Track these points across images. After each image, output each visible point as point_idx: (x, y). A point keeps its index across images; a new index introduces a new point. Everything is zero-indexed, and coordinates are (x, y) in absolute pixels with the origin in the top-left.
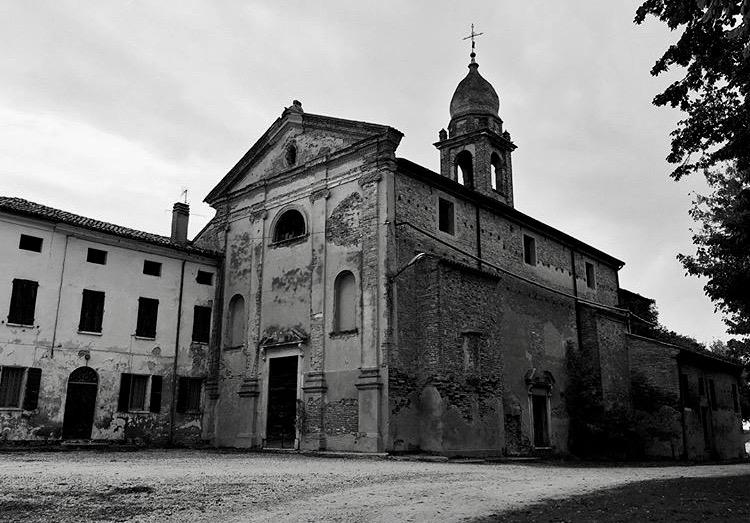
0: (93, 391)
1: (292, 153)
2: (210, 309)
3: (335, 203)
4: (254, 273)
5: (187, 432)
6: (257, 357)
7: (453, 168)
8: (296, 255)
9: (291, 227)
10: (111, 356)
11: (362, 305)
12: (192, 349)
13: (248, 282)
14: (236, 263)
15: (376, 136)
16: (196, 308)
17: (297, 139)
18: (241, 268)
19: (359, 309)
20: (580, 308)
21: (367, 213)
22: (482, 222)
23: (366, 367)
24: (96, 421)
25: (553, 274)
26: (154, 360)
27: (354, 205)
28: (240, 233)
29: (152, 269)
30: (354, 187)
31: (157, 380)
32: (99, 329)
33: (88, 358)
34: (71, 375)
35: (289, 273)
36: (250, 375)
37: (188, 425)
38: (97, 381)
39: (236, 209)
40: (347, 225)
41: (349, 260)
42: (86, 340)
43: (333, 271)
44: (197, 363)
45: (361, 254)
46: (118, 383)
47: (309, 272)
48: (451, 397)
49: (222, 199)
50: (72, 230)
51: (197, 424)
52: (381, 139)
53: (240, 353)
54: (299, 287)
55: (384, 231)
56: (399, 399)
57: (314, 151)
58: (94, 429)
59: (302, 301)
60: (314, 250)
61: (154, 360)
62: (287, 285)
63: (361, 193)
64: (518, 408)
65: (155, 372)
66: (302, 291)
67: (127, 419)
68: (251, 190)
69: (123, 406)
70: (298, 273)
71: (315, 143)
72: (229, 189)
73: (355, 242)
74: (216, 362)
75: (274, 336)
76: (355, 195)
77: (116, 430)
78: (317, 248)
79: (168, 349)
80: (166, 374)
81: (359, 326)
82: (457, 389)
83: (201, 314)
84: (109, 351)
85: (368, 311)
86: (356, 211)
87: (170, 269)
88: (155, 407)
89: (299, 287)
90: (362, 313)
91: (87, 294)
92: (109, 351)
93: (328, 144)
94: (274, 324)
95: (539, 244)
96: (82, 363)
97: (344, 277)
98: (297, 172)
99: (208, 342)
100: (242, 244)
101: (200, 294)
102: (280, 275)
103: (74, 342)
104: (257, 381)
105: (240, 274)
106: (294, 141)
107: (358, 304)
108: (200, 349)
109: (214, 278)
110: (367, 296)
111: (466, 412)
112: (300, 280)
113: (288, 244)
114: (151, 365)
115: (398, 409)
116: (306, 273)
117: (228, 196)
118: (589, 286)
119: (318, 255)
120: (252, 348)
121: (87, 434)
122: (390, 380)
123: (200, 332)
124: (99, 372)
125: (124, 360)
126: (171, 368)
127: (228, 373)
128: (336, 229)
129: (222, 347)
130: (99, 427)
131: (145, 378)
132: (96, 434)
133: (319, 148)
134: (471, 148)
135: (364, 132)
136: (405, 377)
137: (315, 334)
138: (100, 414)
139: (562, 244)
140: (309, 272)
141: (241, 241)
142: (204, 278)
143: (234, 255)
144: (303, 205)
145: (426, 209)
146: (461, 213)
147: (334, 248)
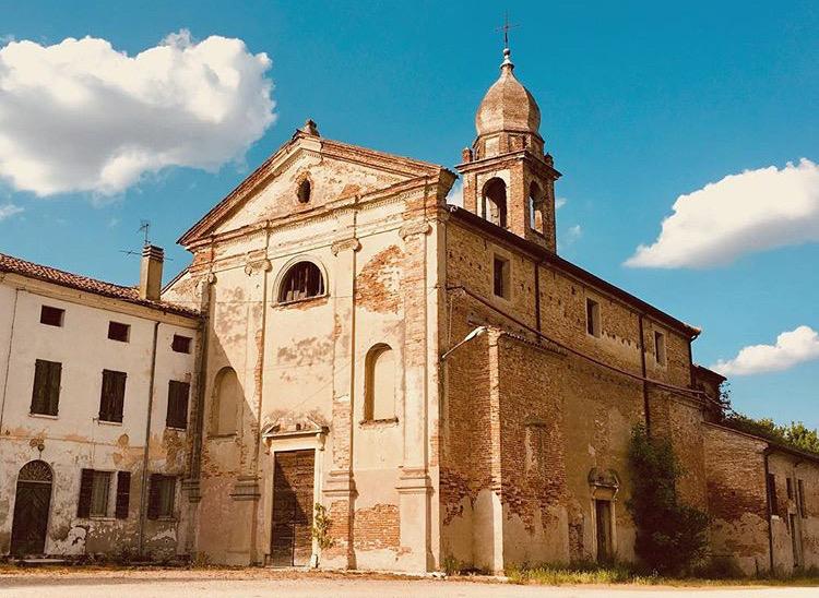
0: (47, 491)
1: (305, 191)
2: (187, 385)
3: (364, 258)
6: (257, 450)
7: (480, 200)
9: (303, 281)
10: (70, 445)
11: (404, 388)
12: (165, 438)
13: (242, 351)
15: (427, 178)
16: (172, 383)
19: (400, 393)
20: (648, 387)
21: (410, 273)
22: (541, 283)
23: (409, 465)
24: (51, 531)
25: (618, 346)
26: (120, 451)
27: (393, 261)
28: (229, 287)
29: (118, 332)
30: (394, 239)
31: (124, 477)
33: (41, 449)
35: (302, 343)
36: (246, 471)
37: (160, 536)
38: (51, 479)
39: (225, 255)
40: (383, 286)
42: (40, 424)
43: (363, 348)
44: (172, 456)
45: (402, 324)
46: (77, 483)
47: (330, 342)
48: (512, 504)
49: (205, 241)
50: (23, 281)
51: (171, 534)
52: (429, 182)
53: (231, 442)
54: (316, 361)
55: (433, 296)
56: (450, 506)
57: (337, 189)
58: (49, 541)
60: (337, 316)
61: (120, 451)
63: (402, 246)
64: (580, 516)
65: (122, 467)
66: (322, 368)
67: (87, 528)
68: (247, 232)
69: (84, 511)
70: (315, 344)
71: (338, 178)
72: (214, 228)
73: (394, 307)
74: (197, 455)
75: (282, 422)
76: (394, 249)
77: (75, 542)
78: (341, 313)
79: (137, 439)
80: (135, 470)
82: (518, 494)
83: (178, 391)
84: (69, 438)
85: (414, 396)
86: (394, 269)
87: (141, 329)
88: (122, 513)
89: (316, 361)
90: (404, 398)
92: (69, 438)
93: (357, 181)
94: (281, 407)
95: (604, 308)
96: (34, 455)
97: (378, 350)
98: (313, 213)
101: (177, 366)
102: (290, 345)
103: (25, 427)
104: (256, 479)
108: (175, 437)
109: (193, 344)
111: (528, 521)
112: (318, 353)
113: (300, 304)
114: (118, 458)
115: (449, 519)
118: (658, 361)
119: (342, 321)
121: (39, 549)
122: (441, 483)
123: (176, 417)
125: (85, 449)
127: (214, 468)
128: (368, 291)
129: (205, 435)
131: (108, 474)
132: (51, 547)
133: (343, 185)
134: (504, 175)
135: (407, 170)
136: (457, 479)
137: (340, 425)
138: (56, 522)
139: (629, 309)
140: (330, 342)
142: (180, 344)
144: (321, 258)
145: (480, 268)
146: (519, 272)
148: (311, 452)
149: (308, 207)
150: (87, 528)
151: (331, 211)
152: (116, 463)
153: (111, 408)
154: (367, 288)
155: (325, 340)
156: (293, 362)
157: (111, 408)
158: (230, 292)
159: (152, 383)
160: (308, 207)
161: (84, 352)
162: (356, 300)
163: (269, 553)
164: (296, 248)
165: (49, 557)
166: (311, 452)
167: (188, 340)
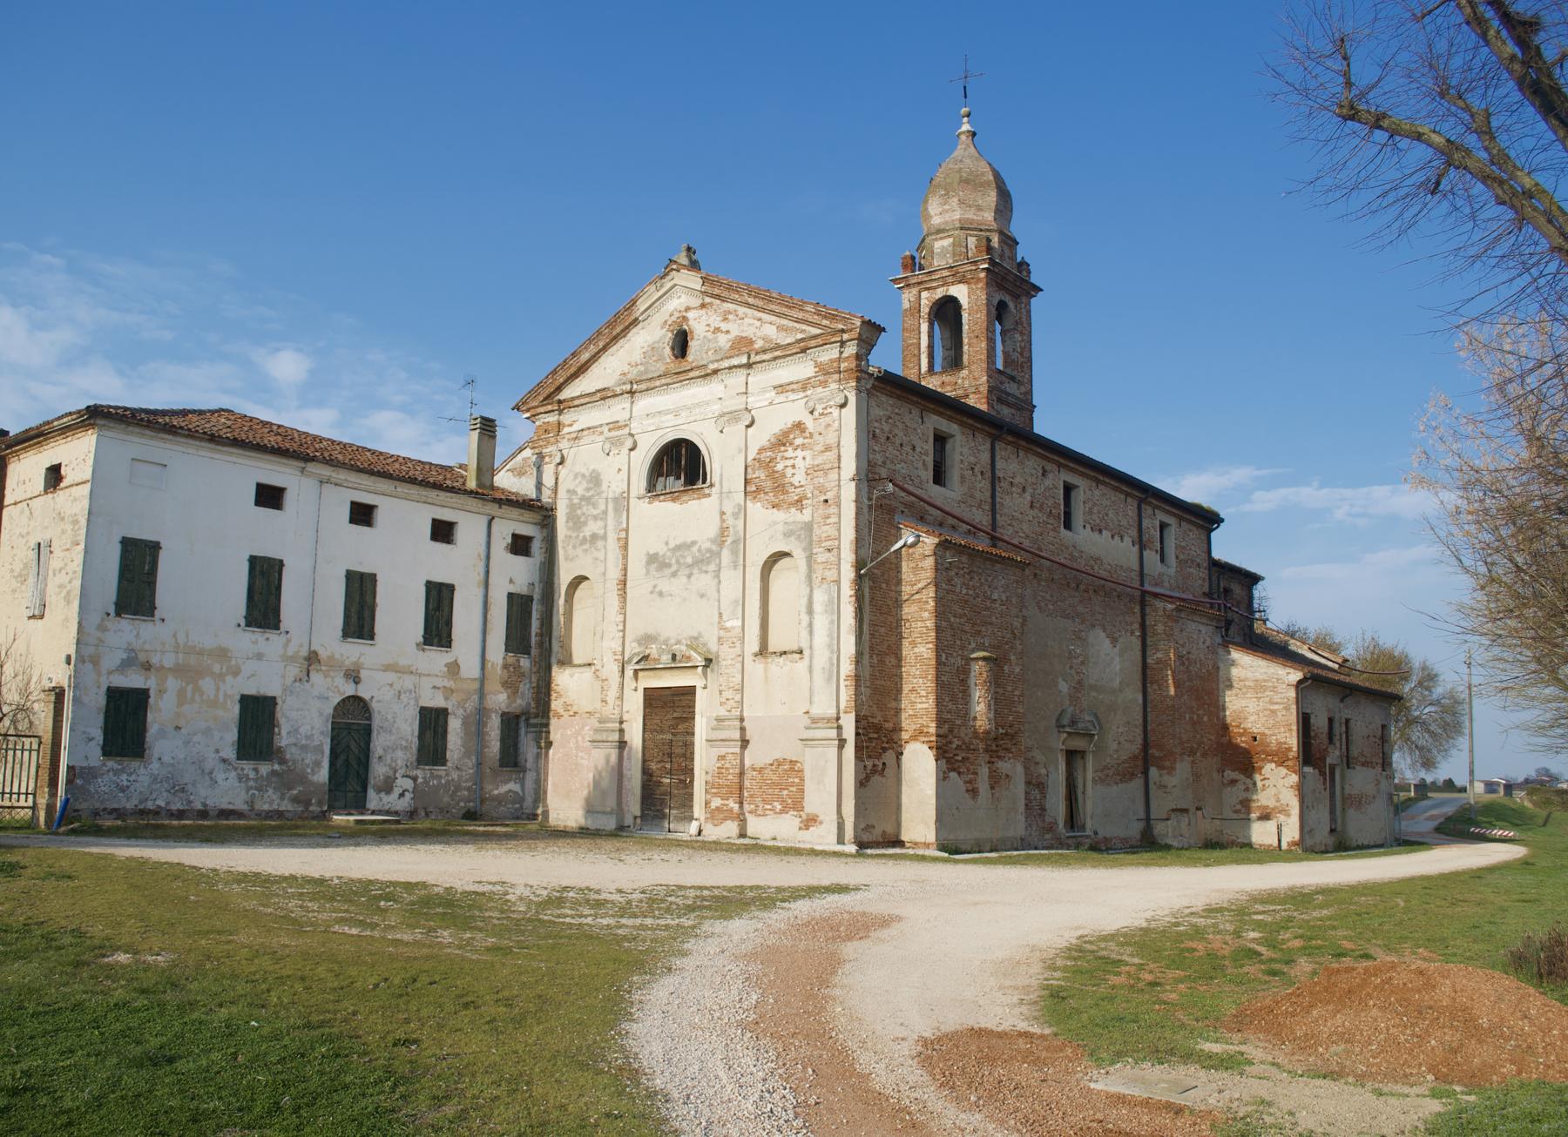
1: (681, 342)
2: (530, 599)
3: (761, 436)
4: (612, 544)
5: (499, 800)
7: (924, 327)
10: (391, 677)
11: (810, 611)
12: (505, 666)
13: (601, 555)
14: (576, 522)
15: (843, 331)
16: (510, 596)
17: (690, 315)
18: (587, 531)
19: (805, 618)
20: (1144, 598)
22: (999, 464)
23: (816, 711)
25: (1104, 543)
26: (450, 684)
28: (583, 470)
29: (443, 532)
32: (372, 637)
33: (357, 681)
34: (335, 709)
35: (678, 548)
37: (503, 789)
38: (369, 718)
39: (576, 427)
40: (784, 476)
41: (787, 535)
42: (354, 651)
43: (757, 556)
45: (809, 527)
47: (714, 548)
48: (949, 761)
49: (550, 408)
50: (326, 471)
53: (587, 674)
55: (849, 492)
56: (869, 763)
57: (723, 341)
58: (371, 793)
59: (702, 596)
60: (723, 513)
62: (674, 568)
63: (809, 422)
64: (1043, 771)
66: (703, 581)
70: (695, 549)
71: (724, 326)
72: (559, 389)
73: (799, 503)
74: (543, 691)
75: (653, 650)
76: (799, 426)
77: (402, 795)
78: (729, 509)
79: (470, 668)
81: (805, 645)
82: (958, 747)
83: (519, 606)
84: (388, 668)
85: (821, 623)
86: (799, 453)
89: (696, 571)
90: (811, 625)
92: (388, 668)
94: (651, 631)
95: (1085, 491)
96: (349, 690)
98: (691, 374)
99: (529, 654)
100: (588, 490)
101: (516, 573)
102: (660, 549)
103: (337, 656)
104: (621, 722)
105: (584, 540)
106: (685, 319)
107: (804, 610)
108: (517, 667)
110: (820, 597)
111: (970, 782)
112: (698, 562)
113: (674, 496)
115: (867, 779)
116: (709, 550)
117: (560, 402)
118: (1162, 560)
119: (730, 521)
120: (612, 670)
121: (360, 805)
122: (857, 734)
123: (517, 640)
124: (374, 705)
126: (476, 697)
127: (567, 706)
128: (765, 481)
130: (379, 791)
132: (374, 799)
134: (960, 292)
136: (878, 728)
137: (727, 655)
138: (378, 771)
139: (1121, 491)
140: (714, 548)
141: (585, 485)
142: (520, 545)
143: (572, 507)
145: (914, 448)
146: (965, 450)
147: (756, 509)
148: (690, 691)
149: (685, 366)
150: (415, 779)
151: (715, 372)
152: (446, 699)
153: (438, 630)
154: (763, 476)
155: (708, 545)
156: (668, 572)
157: (438, 630)
158: (583, 476)
159: (486, 596)
160: (685, 366)
162: (751, 488)
163: (638, 813)
164: (669, 420)
165: (373, 813)
166: (690, 691)
167: (529, 539)
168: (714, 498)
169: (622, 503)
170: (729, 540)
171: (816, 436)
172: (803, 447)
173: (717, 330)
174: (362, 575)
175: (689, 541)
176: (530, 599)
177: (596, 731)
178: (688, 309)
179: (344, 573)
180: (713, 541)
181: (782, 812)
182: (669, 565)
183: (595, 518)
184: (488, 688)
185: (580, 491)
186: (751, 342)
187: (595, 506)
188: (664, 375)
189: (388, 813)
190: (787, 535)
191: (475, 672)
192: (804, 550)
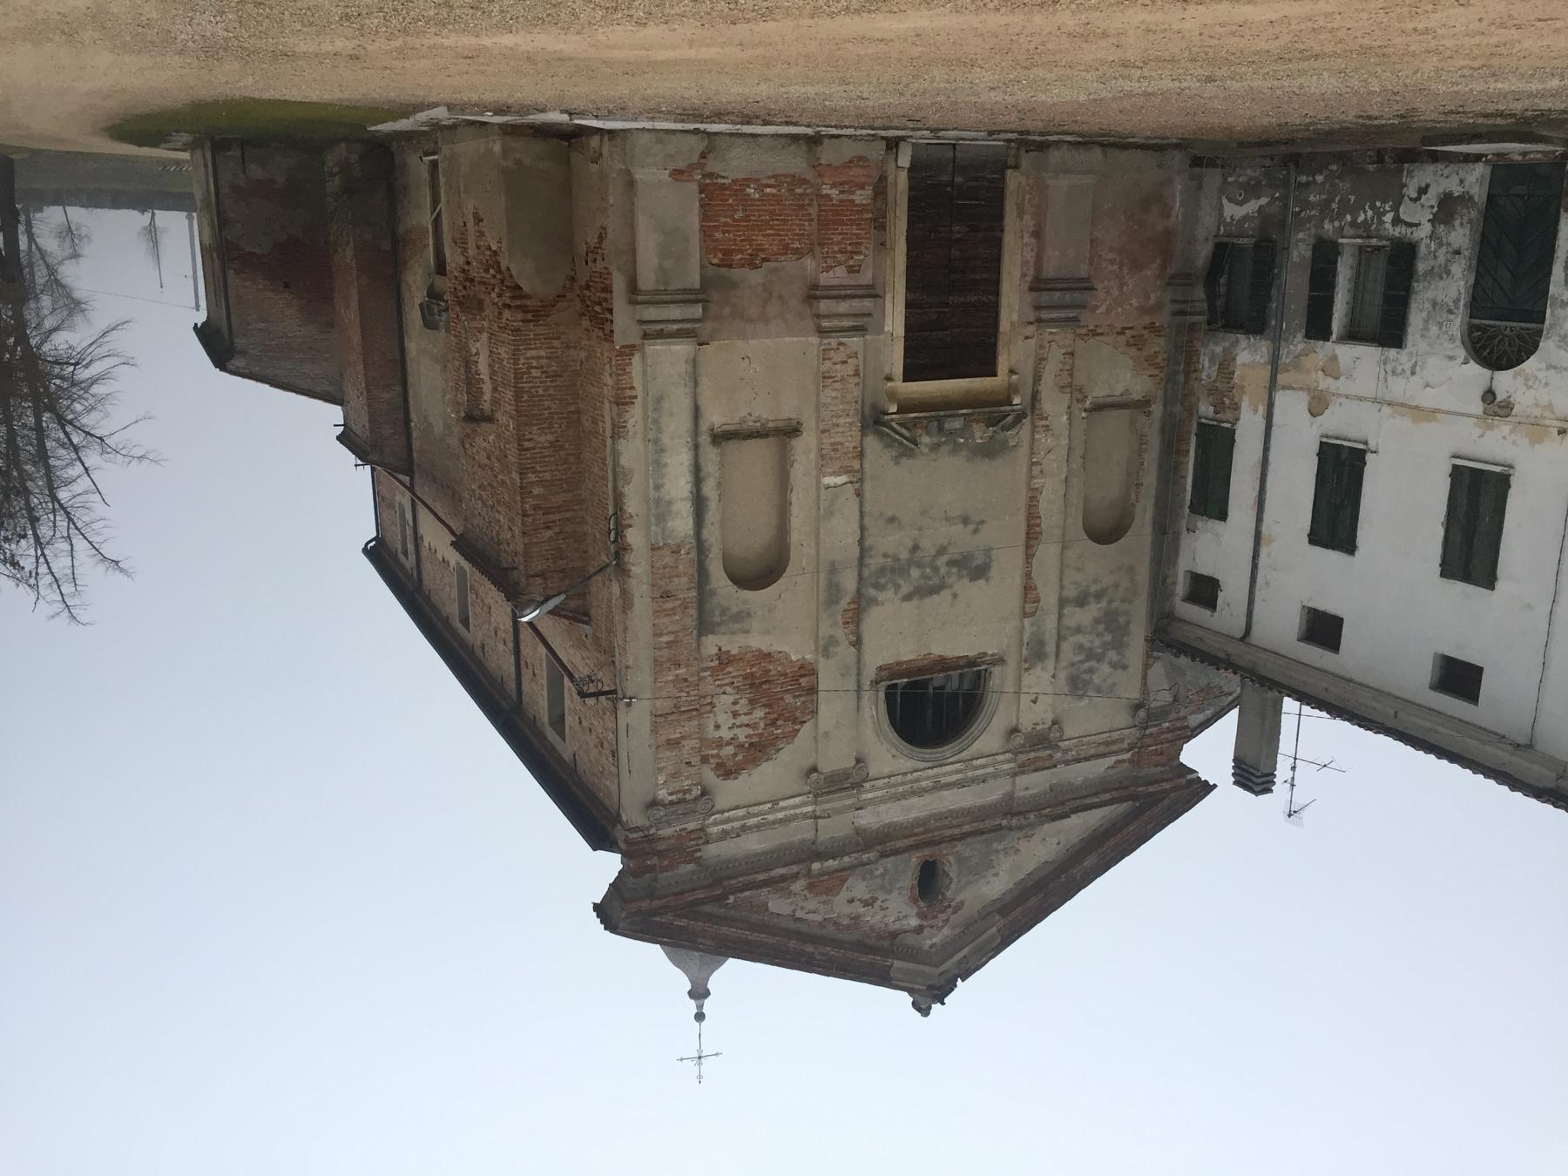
0: (1479, 303)
1: (929, 881)
2: (1194, 509)
4: (1049, 599)
5: (1252, 190)
6: (1037, 378)
8: (901, 634)
9: (931, 707)
10: (1427, 399)
12: (1236, 407)
14: (1113, 624)
15: (656, 912)
16: (1222, 515)
17: (914, 922)
18: (1094, 609)
21: (689, 727)
23: (682, 349)
24: (1474, 214)
27: (730, 750)
30: (729, 793)
31: (1318, 328)
32: (1457, 472)
33: (1489, 395)
34: (1536, 347)
36: (1062, 339)
38: (1472, 328)
40: (751, 701)
41: (743, 616)
42: (1492, 445)
44: (1226, 366)
45: (704, 626)
46: (1416, 319)
47: (872, 592)
50: (1516, 763)
51: (1232, 211)
52: (645, 905)
53: (1098, 392)
54: (904, 555)
57: (858, 887)
58: (1479, 193)
59: (892, 520)
61: (1325, 383)
62: (942, 561)
63: (709, 776)
65: (1324, 349)
66: (890, 543)
67: (1397, 221)
68: (1058, 805)
69: (1403, 257)
70: (906, 589)
73: (724, 660)
74: (1178, 371)
75: (980, 434)
77: (1423, 191)
79: (1291, 406)
80: (1298, 344)
81: (711, 455)
83: (1212, 503)
84: (1431, 414)
86: (725, 734)
87: (1279, 625)
88: (1326, 254)
91: (1488, 579)
92: (1431, 414)
93: (812, 904)
96: (1505, 382)
97: (763, 572)
98: (908, 842)
99: (1200, 425)
100: (1091, 671)
101: (1215, 548)
102: (965, 587)
105: (1098, 596)
106: (921, 916)
107: (713, 506)
108: (1219, 407)
109: (1181, 588)
110: (682, 524)
113: (943, 664)
114: (1332, 369)
116: (880, 588)
117: (1133, 797)
119: (840, 633)
120: (1054, 405)
121: (1503, 173)
123: (1217, 446)
124: (1461, 353)
125: (1399, 388)
126: (1285, 359)
127: (1137, 343)
128: (782, 694)
129: (1157, 409)
130: (1465, 199)
131: (1353, 335)
132: (1474, 181)
133: (844, 895)
135: (699, 925)
137: (847, 433)
138: (1460, 235)
141: (1096, 679)
142: (1205, 590)
143: (1119, 645)
144: (889, 757)
147: (796, 648)
148: (909, 376)
149: (926, 852)
150: (1397, 221)
151: (867, 847)
152: (1334, 358)
153: (1341, 472)
154: (788, 699)
155: (881, 596)
156: (954, 552)
157: (1341, 472)
158: (1098, 690)
159: (1259, 520)
160: (926, 852)
161: (1393, 590)
162: (804, 679)
163: (1009, 172)
164: (949, 773)
165: (1477, 158)
166: (909, 376)
167: (1192, 598)
168: (870, 672)
169: (1036, 654)
170: (844, 604)
171: (695, 760)
172: (720, 743)
173: (868, 903)
174: (1467, 577)
175: (915, 602)
176: (1194, 509)
177: (1083, 306)
178: (919, 930)
179: (1498, 585)
180: (873, 602)
181: (746, 182)
182: (951, 563)
183: (1078, 630)
184: (1265, 373)
185: (1105, 668)
186: (811, 887)
187: (1081, 647)
188: (953, 839)
189: (1080, 135)
190: (743, 616)
191: (1281, 398)
192: (713, 593)
